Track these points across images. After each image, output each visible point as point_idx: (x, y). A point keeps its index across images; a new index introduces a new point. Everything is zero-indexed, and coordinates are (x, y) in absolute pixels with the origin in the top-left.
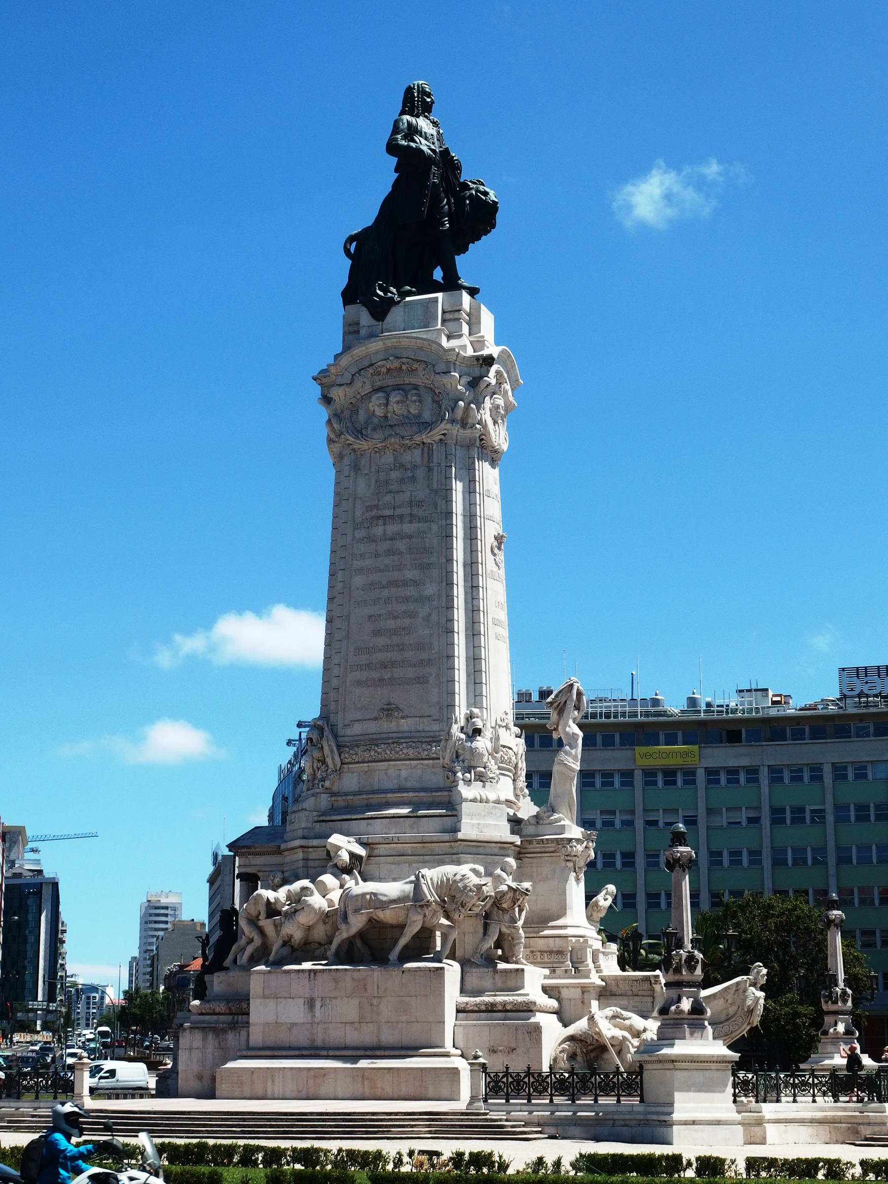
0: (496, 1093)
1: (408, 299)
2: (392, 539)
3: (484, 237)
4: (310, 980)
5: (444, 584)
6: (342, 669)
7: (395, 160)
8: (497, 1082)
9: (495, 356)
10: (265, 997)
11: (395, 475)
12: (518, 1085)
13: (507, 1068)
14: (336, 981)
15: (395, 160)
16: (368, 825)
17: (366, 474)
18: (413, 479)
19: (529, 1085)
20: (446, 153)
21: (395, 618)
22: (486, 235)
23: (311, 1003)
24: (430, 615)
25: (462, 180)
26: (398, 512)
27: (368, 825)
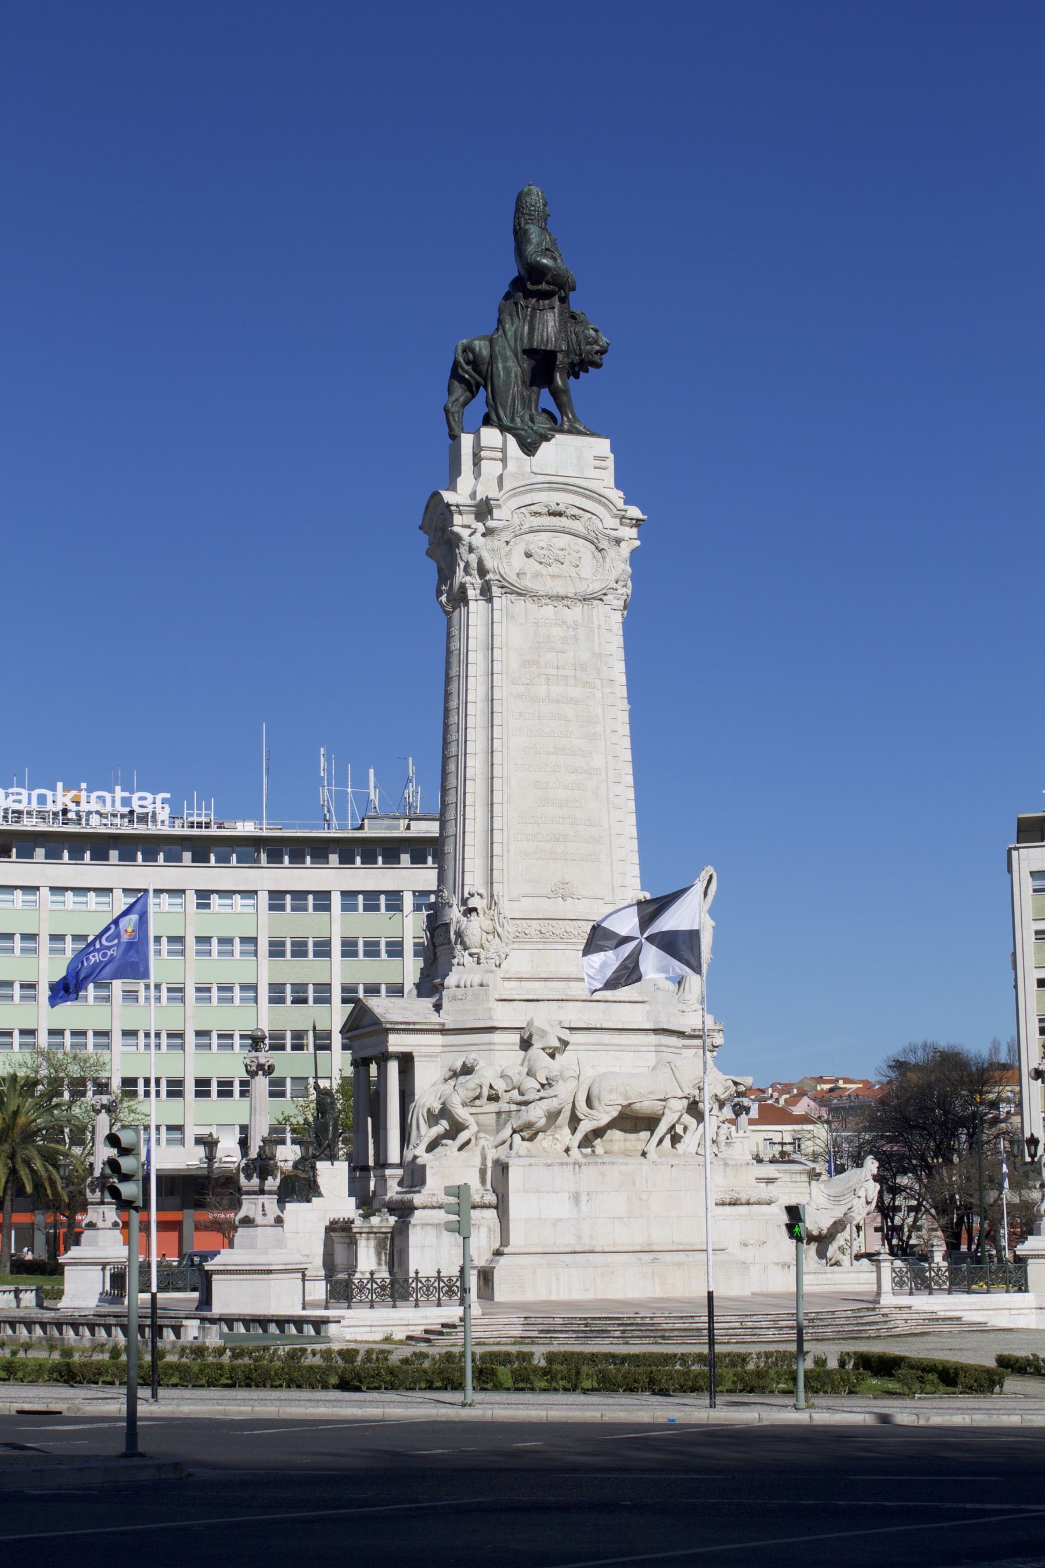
0: (450, 1296)
2: (557, 702)
4: (574, 1174)
5: (610, 758)
6: (505, 835)
8: (901, 1278)
10: (526, 1191)
11: (557, 632)
12: (428, 1290)
13: (439, 1272)
14: (603, 1175)
16: (559, 1007)
17: (521, 624)
18: (576, 638)
19: (372, 1291)
21: (566, 788)
23: (576, 1198)
24: (598, 788)
26: (562, 672)
27: (559, 1007)
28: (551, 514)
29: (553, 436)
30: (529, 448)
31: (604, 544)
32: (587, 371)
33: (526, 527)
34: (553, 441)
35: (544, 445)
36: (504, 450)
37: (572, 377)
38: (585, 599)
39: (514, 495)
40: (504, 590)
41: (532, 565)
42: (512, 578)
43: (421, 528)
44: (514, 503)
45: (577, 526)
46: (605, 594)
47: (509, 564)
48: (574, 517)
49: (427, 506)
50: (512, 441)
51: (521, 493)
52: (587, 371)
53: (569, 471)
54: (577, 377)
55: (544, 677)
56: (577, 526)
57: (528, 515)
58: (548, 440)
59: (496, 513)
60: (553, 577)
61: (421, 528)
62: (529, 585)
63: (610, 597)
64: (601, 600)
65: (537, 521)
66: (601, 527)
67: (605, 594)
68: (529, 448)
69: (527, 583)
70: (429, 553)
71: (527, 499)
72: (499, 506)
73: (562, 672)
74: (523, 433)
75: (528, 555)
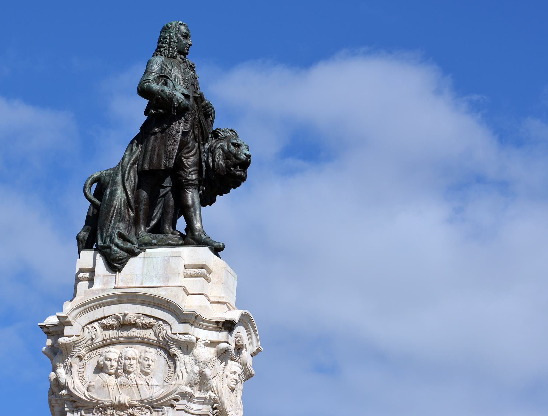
1: (148, 250)
3: (232, 190)
7: (145, 102)
9: (237, 320)
15: (145, 102)
20: (199, 99)
22: (235, 188)
25: (214, 128)
29: (144, 250)
30: (114, 265)
31: (175, 350)
33: (98, 340)
34: (141, 255)
35: (132, 260)
36: (92, 271)
39: (85, 311)
45: (149, 334)
46: (176, 400)
48: (145, 327)
50: (100, 262)
56: (149, 334)
59: (67, 330)
62: (95, 396)
64: (172, 406)
66: (169, 332)
68: (114, 265)
72: (69, 324)
74: (108, 250)
75: (100, 369)
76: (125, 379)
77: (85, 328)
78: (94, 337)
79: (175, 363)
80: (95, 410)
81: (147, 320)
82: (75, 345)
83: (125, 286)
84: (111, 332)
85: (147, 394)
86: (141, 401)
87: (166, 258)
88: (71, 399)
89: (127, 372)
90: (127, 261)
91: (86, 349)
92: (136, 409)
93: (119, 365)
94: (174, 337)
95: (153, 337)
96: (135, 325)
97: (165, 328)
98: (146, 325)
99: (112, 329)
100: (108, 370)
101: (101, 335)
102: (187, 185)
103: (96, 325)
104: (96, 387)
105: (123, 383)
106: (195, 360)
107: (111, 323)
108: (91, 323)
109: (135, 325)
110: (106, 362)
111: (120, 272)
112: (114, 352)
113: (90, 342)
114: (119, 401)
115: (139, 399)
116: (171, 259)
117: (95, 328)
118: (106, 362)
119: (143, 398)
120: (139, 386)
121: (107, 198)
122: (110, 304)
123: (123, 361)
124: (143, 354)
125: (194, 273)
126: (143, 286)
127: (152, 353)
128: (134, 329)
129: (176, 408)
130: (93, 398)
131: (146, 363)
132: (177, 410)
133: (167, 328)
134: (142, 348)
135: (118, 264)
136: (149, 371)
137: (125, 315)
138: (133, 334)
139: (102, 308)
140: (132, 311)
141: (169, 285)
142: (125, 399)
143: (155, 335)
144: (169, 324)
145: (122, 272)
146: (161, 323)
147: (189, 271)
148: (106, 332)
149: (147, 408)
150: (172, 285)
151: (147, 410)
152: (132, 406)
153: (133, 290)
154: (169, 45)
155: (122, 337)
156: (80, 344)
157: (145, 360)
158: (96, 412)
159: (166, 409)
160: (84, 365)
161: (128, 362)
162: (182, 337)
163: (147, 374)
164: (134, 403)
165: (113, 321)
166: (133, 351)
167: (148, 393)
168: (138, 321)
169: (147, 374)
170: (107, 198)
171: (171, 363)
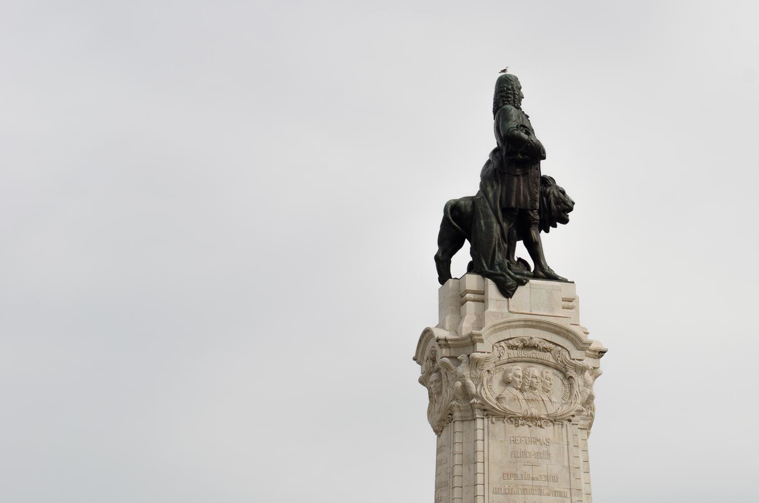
11: (531, 448)
17: (501, 441)
28: (526, 347)
29: (527, 281)
30: (507, 291)
31: (572, 373)
32: (555, 226)
33: (505, 358)
34: (527, 285)
35: (520, 288)
37: (543, 232)
38: (554, 420)
39: (495, 331)
40: (485, 413)
41: (510, 392)
42: (493, 402)
43: (415, 359)
44: (494, 339)
45: (548, 357)
46: (573, 416)
47: (490, 389)
48: (545, 350)
49: (420, 341)
51: (500, 330)
52: (555, 226)
53: (542, 312)
54: (547, 231)
55: (521, 487)
56: (548, 357)
57: (506, 348)
58: (524, 284)
59: (479, 346)
60: (528, 400)
61: (415, 359)
62: (508, 407)
63: (577, 418)
64: (570, 421)
65: (514, 353)
66: (569, 359)
67: (573, 416)
68: (507, 291)
69: (507, 406)
70: (422, 381)
71: (506, 334)
72: (482, 341)
73: (536, 483)
74: (502, 278)
75: (506, 383)
76: (531, 394)
77: (495, 347)
78: (502, 355)
79: (571, 385)
80: (506, 419)
81: (547, 345)
82: (486, 360)
83: (516, 311)
84: (515, 351)
85: (552, 409)
86: (548, 415)
87: (549, 291)
88: (483, 407)
89: (532, 388)
90: (516, 289)
91: (494, 365)
92: (543, 421)
93: (526, 382)
94: (571, 361)
95: (552, 360)
96: (535, 347)
97: (564, 353)
98: (546, 349)
99: (517, 349)
100: (517, 385)
101: (508, 354)
102: (534, 224)
103: (503, 344)
104: (507, 399)
105: (530, 398)
106: (585, 383)
107: (517, 344)
108: (499, 342)
109: (535, 347)
110: (515, 378)
111: (511, 298)
112: (518, 369)
113: (498, 359)
114: (532, 414)
115: (547, 413)
116: (553, 292)
117: (503, 347)
118: (515, 378)
119: (549, 413)
120: (545, 402)
121: (484, 228)
122: (517, 327)
123: (530, 379)
124: (545, 374)
125: (567, 305)
126: (533, 313)
127: (550, 373)
128: (534, 351)
129: (572, 423)
130: (506, 409)
131: (549, 382)
132: (573, 424)
133: (564, 353)
134: (541, 367)
135: (510, 291)
136: (550, 389)
137: (531, 338)
138: (534, 355)
139: (508, 330)
140: (537, 336)
141: (555, 315)
142: (535, 412)
143: (554, 358)
144: (567, 350)
145: (513, 297)
146: (560, 348)
147: (564, 303)
148: (511, 351)
149: (551, 421)
150: (537, 313)
151: (551, 423)
152: (540, 419)
153: (538, 318)
154: (514, 97)
155: (524, 357)
156: (490, 360)
157: (547, 379)
158: (507, 421)
159: (566, 422)
160: (491, 379)
161: (535, 380)
162: (580, 362)
163: (548, 391)
164: (543, 416)
165: (518, 342)
166: (536, 370)
167: (552, 409)
168: (540, 344)
169: (548, 391)
170: (484, 228)
171: (566, 382)
